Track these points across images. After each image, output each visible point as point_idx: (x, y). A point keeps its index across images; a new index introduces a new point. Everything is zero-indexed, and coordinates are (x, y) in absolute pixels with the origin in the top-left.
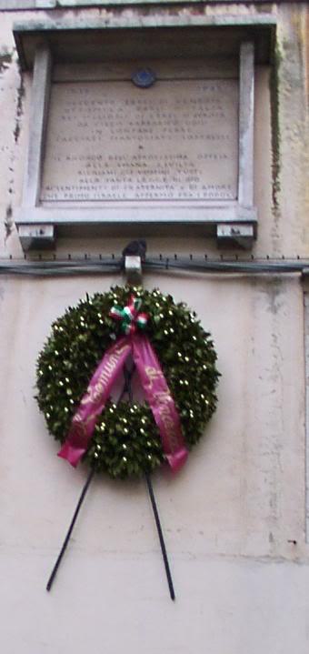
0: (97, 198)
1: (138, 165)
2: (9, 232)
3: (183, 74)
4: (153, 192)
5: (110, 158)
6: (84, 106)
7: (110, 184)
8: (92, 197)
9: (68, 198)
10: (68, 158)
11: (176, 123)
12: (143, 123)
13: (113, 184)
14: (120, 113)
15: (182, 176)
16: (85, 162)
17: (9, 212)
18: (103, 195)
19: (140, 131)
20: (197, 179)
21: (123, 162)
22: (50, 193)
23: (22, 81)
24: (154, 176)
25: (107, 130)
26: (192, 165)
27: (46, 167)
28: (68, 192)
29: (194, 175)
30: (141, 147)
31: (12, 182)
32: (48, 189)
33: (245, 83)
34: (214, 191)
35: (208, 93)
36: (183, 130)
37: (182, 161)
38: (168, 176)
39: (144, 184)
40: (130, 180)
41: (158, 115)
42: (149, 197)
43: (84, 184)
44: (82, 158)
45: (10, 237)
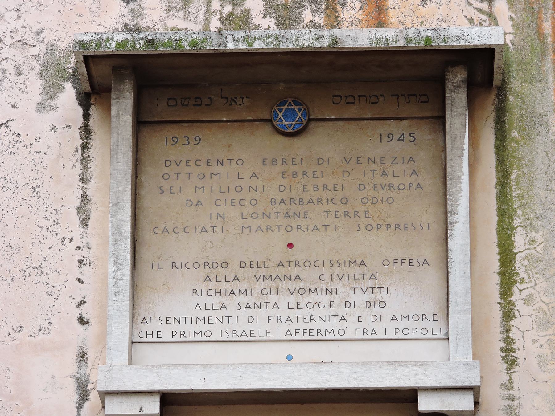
0: (224, 338)
1: (289, 278)
2: (83, 397)
3: (352, 111)
4: (314, 326)
5: (242, 265)
6: (192, 168)
7: (245, 313)
8: (216, 336)
9: (177, 338)
10: (174, 265)
11: (345, 201)
12: (292, 200)
13: (249, 312)
14: (255, 182)
15: (360, 298)
16: (202, 273)
17: (82, 356)
18: (234, 333)
19: (287, 215)
20: (383, 304)
21: (263, 272)
22: (145, 328)
23: (86, 116)
24: (314, 298)
25: (233, 213)
26: (373, 277)
27: (136, 279)
28: (178, 327)
29: (379, 297)
30: (290, 245)
31: (82, 303)
32: (144, 320)
33: (454, 139)
34: (410, 324)
35: (395, 146)
36: (356, 214)
37: (357, 271)
38: (336, 299)
39: (298, 312)
40: (276, 305)
41: (316, 187)
42: (307, 337)
43: (202, 314)
44: (196, 265)
45: (87, 405)
